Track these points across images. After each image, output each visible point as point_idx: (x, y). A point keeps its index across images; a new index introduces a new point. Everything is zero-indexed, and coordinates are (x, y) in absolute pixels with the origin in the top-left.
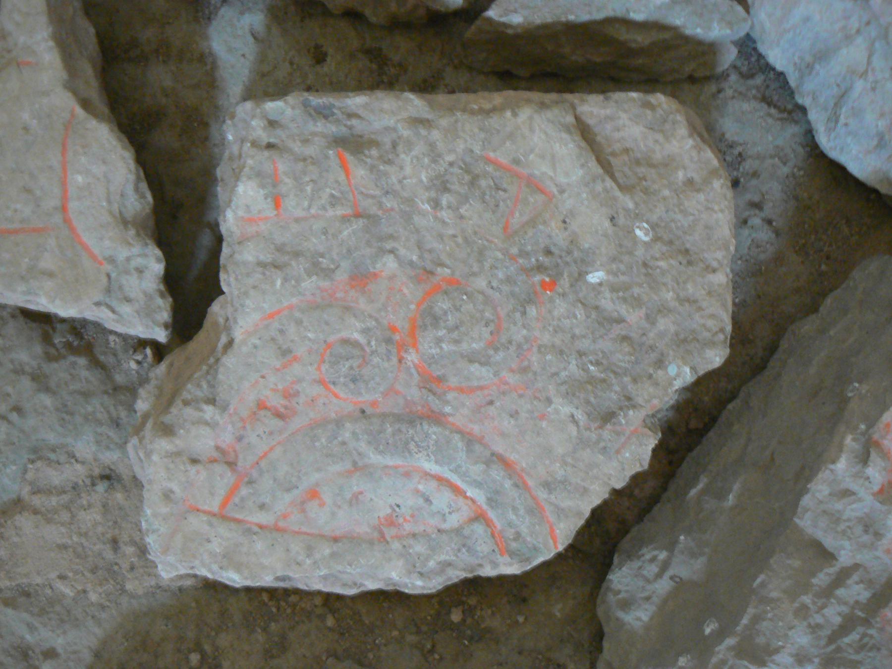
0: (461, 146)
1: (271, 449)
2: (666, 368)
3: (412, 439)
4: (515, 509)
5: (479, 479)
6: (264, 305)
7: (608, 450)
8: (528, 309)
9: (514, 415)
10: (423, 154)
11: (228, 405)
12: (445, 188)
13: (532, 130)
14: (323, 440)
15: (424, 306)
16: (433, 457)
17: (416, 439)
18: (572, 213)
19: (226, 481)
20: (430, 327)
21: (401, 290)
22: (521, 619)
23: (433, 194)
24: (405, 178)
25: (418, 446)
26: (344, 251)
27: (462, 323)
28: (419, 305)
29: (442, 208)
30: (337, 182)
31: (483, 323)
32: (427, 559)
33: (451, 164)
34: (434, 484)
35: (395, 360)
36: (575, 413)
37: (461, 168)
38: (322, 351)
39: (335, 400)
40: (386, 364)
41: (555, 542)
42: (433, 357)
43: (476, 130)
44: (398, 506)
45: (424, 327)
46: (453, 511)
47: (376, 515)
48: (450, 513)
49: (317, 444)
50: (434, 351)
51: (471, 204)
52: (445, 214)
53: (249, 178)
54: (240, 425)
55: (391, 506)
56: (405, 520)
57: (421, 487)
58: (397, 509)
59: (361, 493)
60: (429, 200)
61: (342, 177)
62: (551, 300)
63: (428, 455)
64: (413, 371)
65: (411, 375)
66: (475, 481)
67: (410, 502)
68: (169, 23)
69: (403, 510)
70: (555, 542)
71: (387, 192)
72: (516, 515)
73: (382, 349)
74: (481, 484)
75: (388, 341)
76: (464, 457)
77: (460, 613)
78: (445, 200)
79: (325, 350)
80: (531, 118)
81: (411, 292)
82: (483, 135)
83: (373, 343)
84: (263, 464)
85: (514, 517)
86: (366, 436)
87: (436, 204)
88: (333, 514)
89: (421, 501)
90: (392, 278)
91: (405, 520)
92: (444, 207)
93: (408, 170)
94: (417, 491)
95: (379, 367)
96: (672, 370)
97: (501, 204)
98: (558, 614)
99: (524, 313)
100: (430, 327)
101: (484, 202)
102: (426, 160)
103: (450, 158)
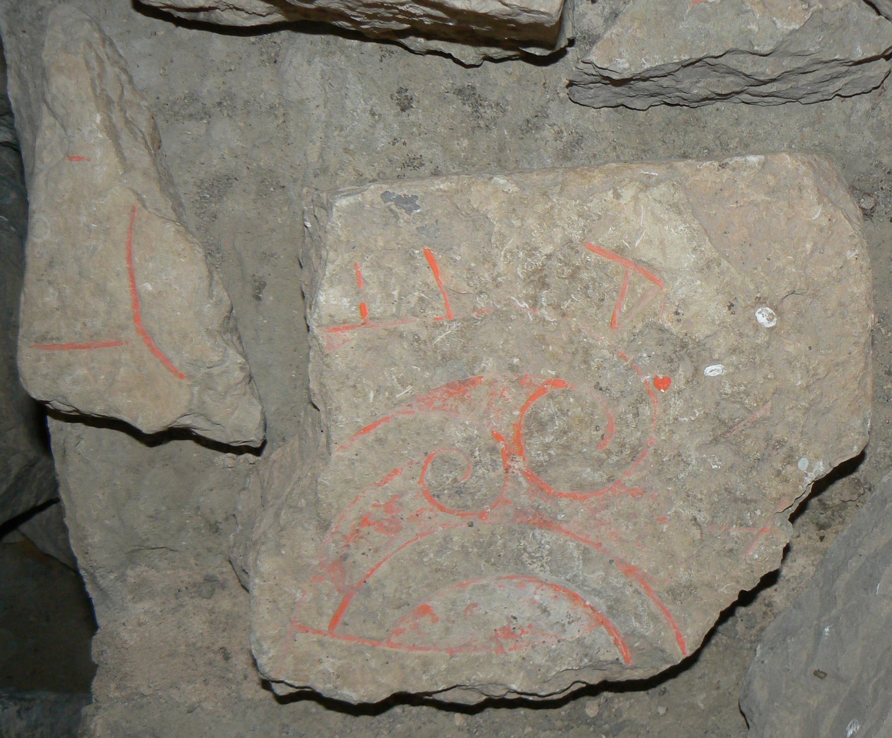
0: (558, 237)
1: (379, 565)
2: (797, 462)
3: (525, 549)
4: (638, 617)
5: (598, 588)
6: (358, 420)
7: (735, 552)
8: (640, 410)
9: (632, 516)
10: (517, 247)
11: (329, 525)
12: (543, 284)
13: (637, 213)
14: (432, 555)
15: (528, 412)
16: (548, 568)
17: (529, 550)
18: (684, 302)
19: (333, 600)
20: (536, 434)
21: (502, 396)
22: (662, 710)
23: (531, 292)
24: (499, 275)
25: (531, 557)
26: (439, 358)
27: (570, 428)
28: (523, 410)
29: (542, 306)
30: (426, 284)
31: (593, 427)
32: (549, 669)
33: (549, 257)
34: (551, 593)
35: (501, 470)
36: (698, 517)
37: (560, 261)
38: (423, 463)
39: (441, 514)
40: (492, 475)
41: (683, 648)
42: (542, 465)
43: (575, 218)
44: (515, 618)
45: (531, 434)
46: (573, 621)
47: (493, 628)
48: (569, 623)
49: (425, 560)
50: (541, 458)
51: (573, 300)
52: (545, 313)
53: (332, 285)
54: (342, 544)
55: (507, 618)
56: (523, 631)
57: (537, 598)
58: (514, 621)
59: (475, 605)
60: (526, 298)
61: (431, 279)
62: (665, 399)
63: (542, 566)
64: (521, 479)
65: (520, 484)
66: (594, 589)
67: (525, 613)
68: (231, 70)
69: (520, 621)
70: (683, 648)
71: (481, 292)
72: (640, 623)
73: (487, 458)
74: (600, 592)
75: (493, 450)
76: (581, 567)
77: (596, 707)
78: (544, 296)
79: (426, 462)
80: (635, 198)
81: (514, 397)
82: (582, 222)
83: (477, 453)
84: (370, 580)
85: (638, 625)
86: (476, 550)
87: (535, 302)
88: (447, 630)
89: (538, 612)
90: (492, 383)
91: (523, 631)
92: (545, 304)
93: (502, 267)
94: (533, 602)
95: (484, 478)
96: (803, 464)
97: (607, 297)
98: (701, 706)
99: (637, 415)
100: (536, 434)
101: (588, 297)
102: (521, 254)
103: (549, 249)
